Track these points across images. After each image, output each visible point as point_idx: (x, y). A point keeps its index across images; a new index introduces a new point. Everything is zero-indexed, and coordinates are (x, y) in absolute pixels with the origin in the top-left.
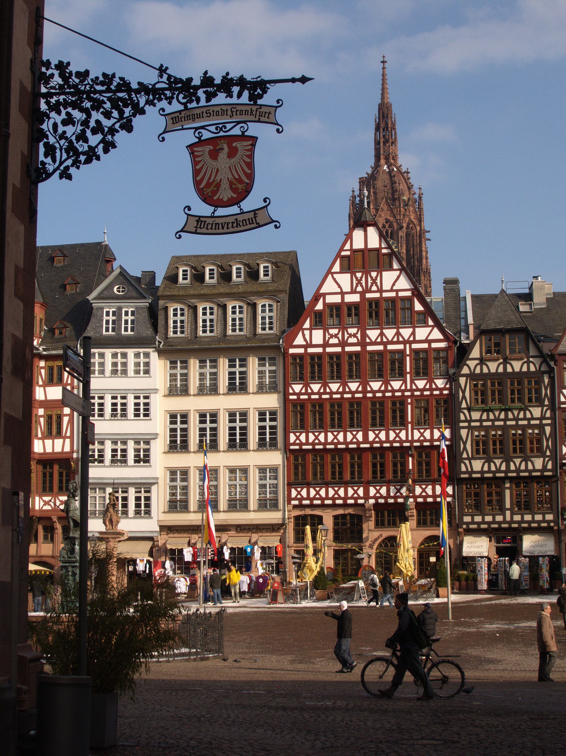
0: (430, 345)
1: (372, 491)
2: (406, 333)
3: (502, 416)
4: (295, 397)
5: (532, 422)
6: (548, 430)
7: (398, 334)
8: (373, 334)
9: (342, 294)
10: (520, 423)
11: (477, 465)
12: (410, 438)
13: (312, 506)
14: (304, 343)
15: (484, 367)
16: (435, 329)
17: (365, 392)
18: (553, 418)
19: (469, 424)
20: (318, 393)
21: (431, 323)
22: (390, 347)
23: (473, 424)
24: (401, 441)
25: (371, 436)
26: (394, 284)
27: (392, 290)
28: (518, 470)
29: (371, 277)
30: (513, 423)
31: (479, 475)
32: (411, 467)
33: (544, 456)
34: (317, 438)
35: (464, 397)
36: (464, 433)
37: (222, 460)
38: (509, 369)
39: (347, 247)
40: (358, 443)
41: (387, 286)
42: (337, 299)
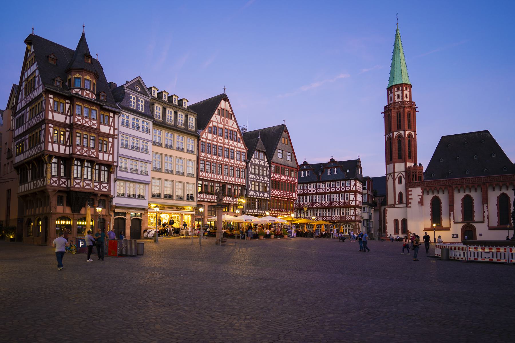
2: (235, 143)
8: (226, 141)
9: (218, 123)
18: (269, 181)
20: (210, 158)
21: (242, 142)
22: (231, 147)
24: (232, 182)
25: (225, 178)
28: (262, 196)
33: (267, 192)
36: (249, 181)
39: (220, 106)
40: (221, 180)
41: (230, 125)
42: (216, 124)
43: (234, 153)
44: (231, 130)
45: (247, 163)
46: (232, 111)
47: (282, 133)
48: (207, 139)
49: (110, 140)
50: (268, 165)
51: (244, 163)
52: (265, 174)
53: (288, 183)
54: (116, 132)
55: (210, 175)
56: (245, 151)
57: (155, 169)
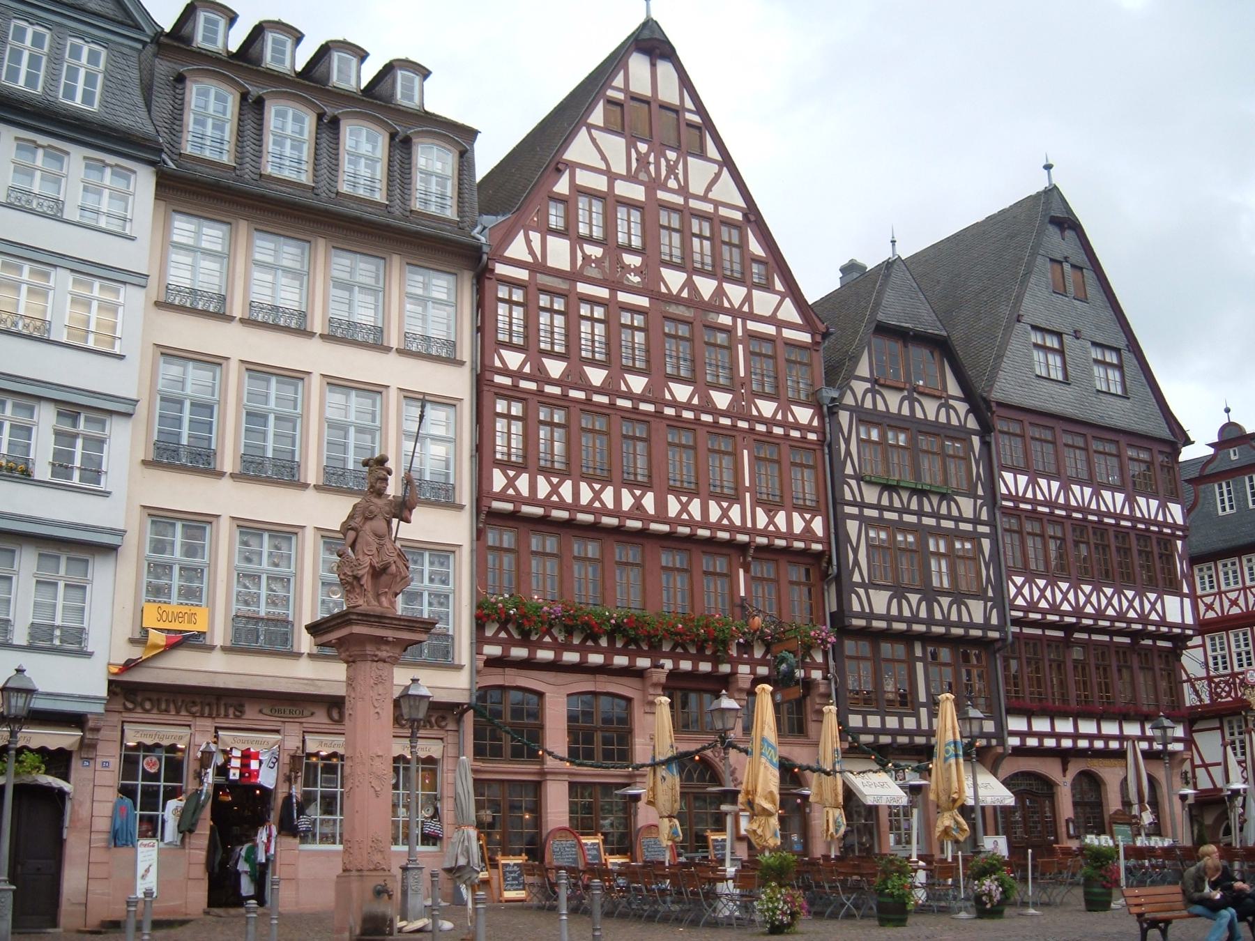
0: (779, 332)
2: (735, 293)
3: (914, 506)
4: (507, 381)
5: (963, 526)
6: (986, 543)
7: (719, 292)
8: (674, 280)
10: (944, 523)
11: (880, 601)
12: (749, 525)
13: (528, 664)
14: (530, 259)
15: (878, 397)
16: (788, 302)
18: (991, 523)
19: (861, 512)
21: (779, 286)
23: (867, 512)
24: (731, 528)
25: (673, 507)
26: (709, 189)
27: (704, 198)
28: (946, 622)
29: (668, 161)
30: (931, 522)
31: (881, 625)
32: (742, 594)
34: (555, 489)
35: (848, 453)
36: (852, 527)
38: (919, 414)
39: (619, 81)
41: (697, 187)
43: (730, 348)
44: (702, 216)
45: (827, 412)
46: (701, 109)
47: (1041, 233)
48: (538, 266)
50: (972, 423)
51: (804, 415)
53: (1122, 533)
55: (566, 490)
56: (806, 337)
57: (166, 456)
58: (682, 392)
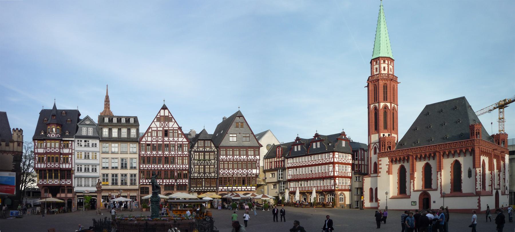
1: (165, 181)
6: (216, 166)
11: (196, 175)
17: (163, 154)
18: (217, 163)
36: (192, 166)
37: (119, 172)
45: (190, 152)
49: (70, 156)
50: (216, 150)
52: (212, 157)
54: (73, 151)
58: (167, 153)
